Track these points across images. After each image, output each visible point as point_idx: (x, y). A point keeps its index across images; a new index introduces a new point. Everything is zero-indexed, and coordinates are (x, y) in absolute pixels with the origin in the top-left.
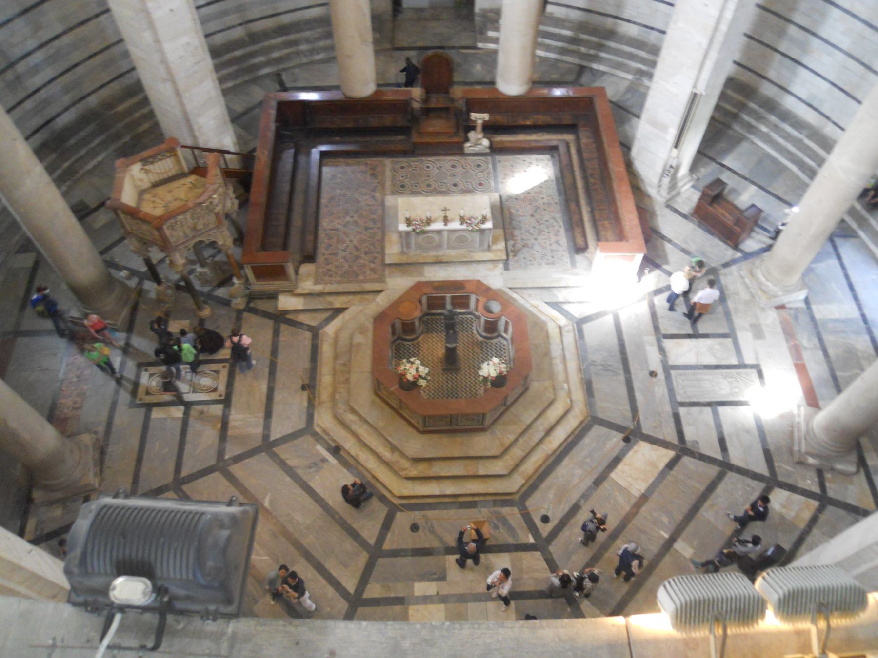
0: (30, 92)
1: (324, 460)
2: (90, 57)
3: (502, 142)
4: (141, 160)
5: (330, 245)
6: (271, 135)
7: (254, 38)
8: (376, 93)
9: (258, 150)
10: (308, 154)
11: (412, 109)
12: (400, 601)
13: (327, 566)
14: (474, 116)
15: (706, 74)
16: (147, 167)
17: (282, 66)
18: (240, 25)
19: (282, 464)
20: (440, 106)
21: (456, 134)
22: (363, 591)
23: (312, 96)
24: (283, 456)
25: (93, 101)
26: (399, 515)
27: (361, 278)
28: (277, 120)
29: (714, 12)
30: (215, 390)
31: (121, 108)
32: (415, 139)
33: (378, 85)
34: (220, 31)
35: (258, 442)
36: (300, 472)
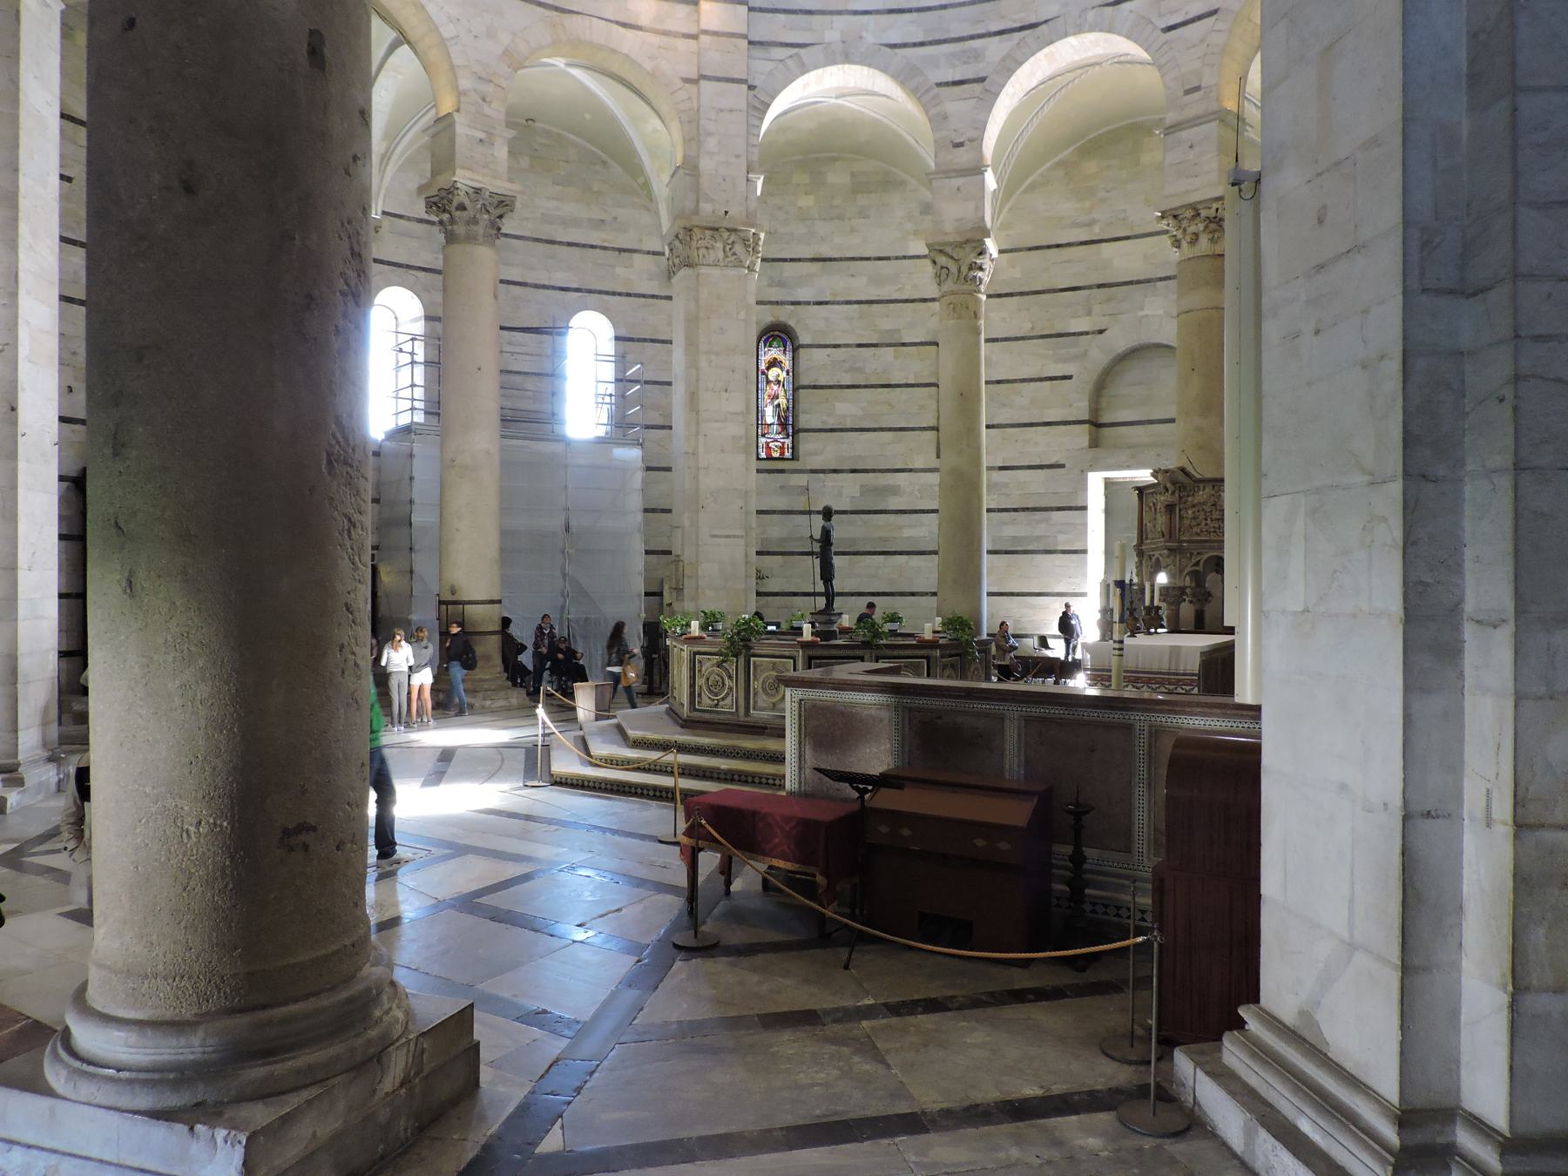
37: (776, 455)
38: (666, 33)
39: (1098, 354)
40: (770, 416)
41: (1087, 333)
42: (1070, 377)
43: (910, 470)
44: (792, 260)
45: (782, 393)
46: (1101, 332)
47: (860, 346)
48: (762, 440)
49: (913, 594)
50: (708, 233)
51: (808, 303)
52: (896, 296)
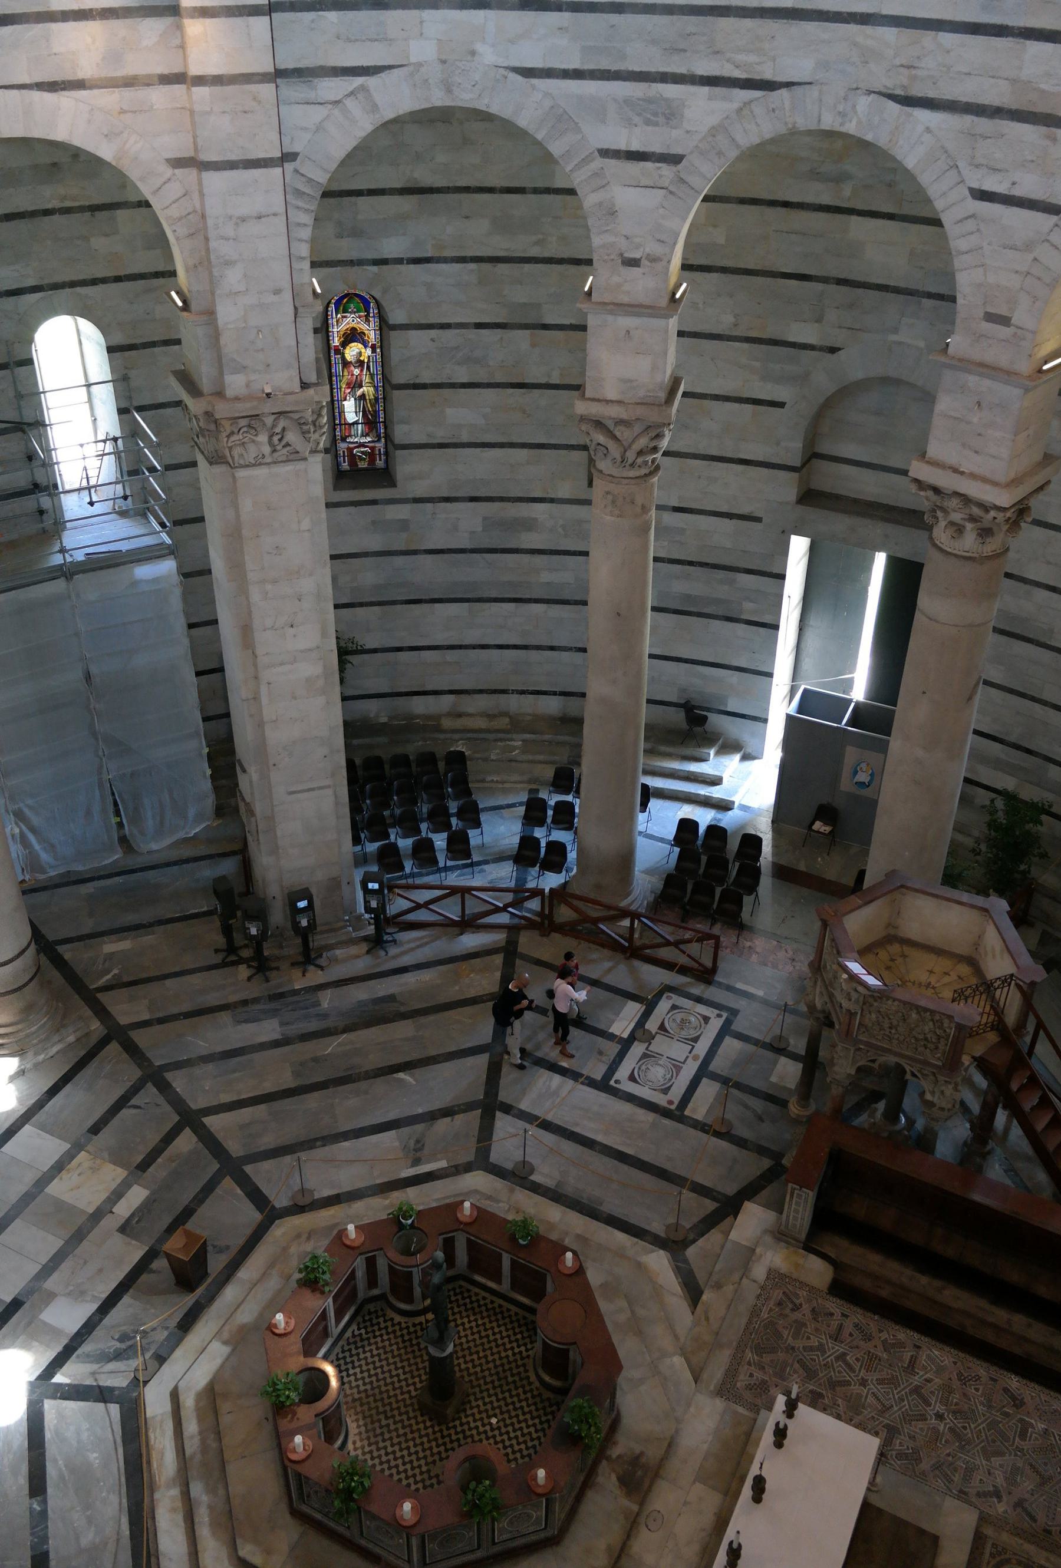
1: (416, 1162)
5: (868, 1338)
12: (144, 1166)
13: (263, 1107)
19: (448, 1112)
22: (195, 1132)
24: (459, 1119)
26: (257, 1216)
27: (749, 1355)
30: (632, 1078)
35: (503, 1096)
36: (419, 1128)
37: (363, 465)
38: (130, 82)
39: (823, 379)
40: (350, 410)
41: (812, 347)
42: (781, 405)
43: (552, 501)
44: (372, 192)
45: (366, 379)
46: (833, 350)
47: (479, 326)
48: (342, 446)
49: (552, 648)
50: (243, 422)
51: (399, 261)
52: (535, 252)
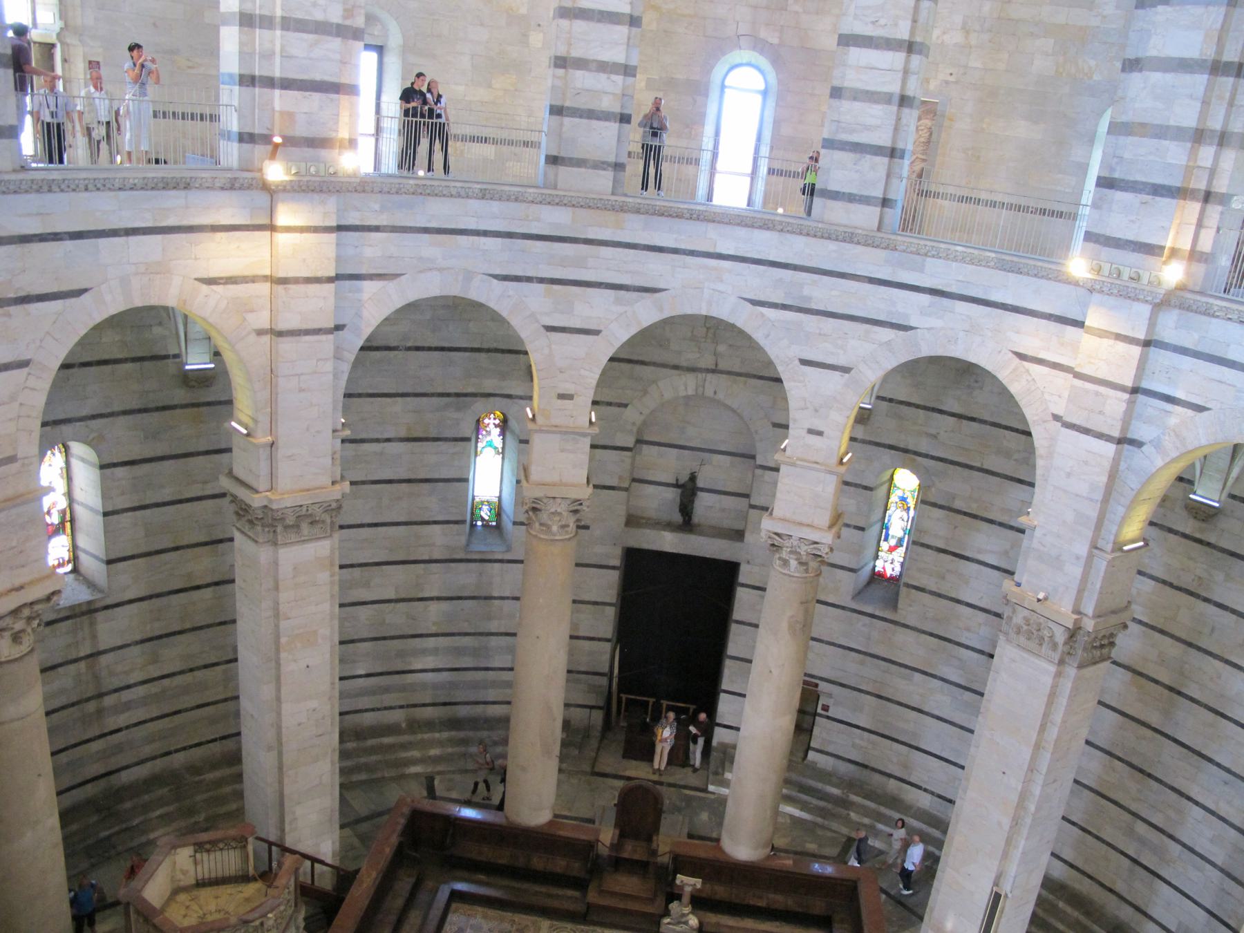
0: (106, 731)
2: (199, 707)
3: (718, 924)
4: (195, 844)
6: (388, 851)
7: (414, 726)
8: (550, 823)
9: (363, 871)
10: (435, 891)
11: (598, 856)
14: (680, 878)
15: (1012, 869)
16: (198, 855)
17: (439, 768)
18: (401, 707)
20: (636, 857)
21: (651, 900)
23: (469, 813)
25: (179, 759)
28: (403, 833)
29: (1015, 783)
31: (210, 776)
32: (592, 896)
33: (556, 816)
34: (373, 710)
